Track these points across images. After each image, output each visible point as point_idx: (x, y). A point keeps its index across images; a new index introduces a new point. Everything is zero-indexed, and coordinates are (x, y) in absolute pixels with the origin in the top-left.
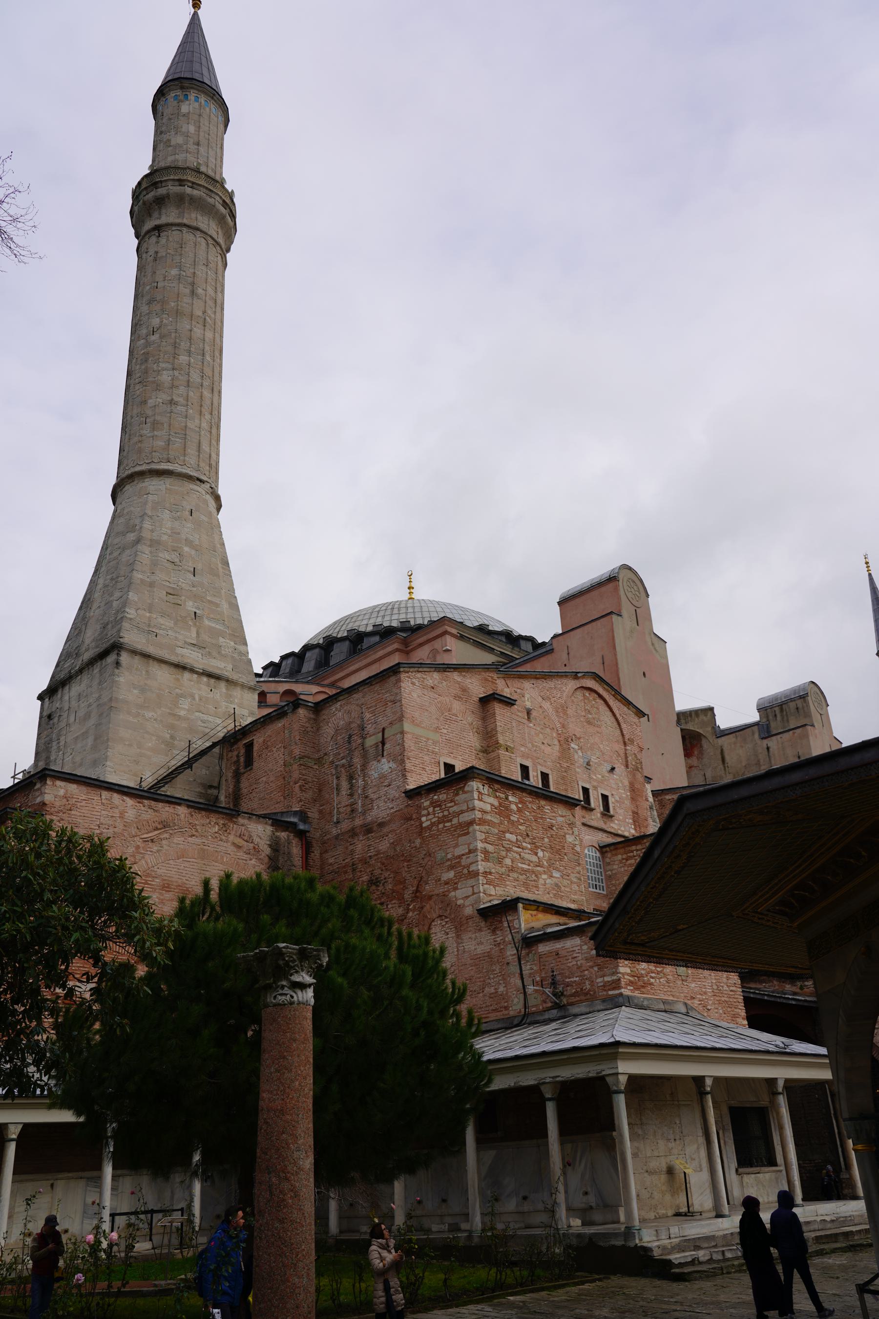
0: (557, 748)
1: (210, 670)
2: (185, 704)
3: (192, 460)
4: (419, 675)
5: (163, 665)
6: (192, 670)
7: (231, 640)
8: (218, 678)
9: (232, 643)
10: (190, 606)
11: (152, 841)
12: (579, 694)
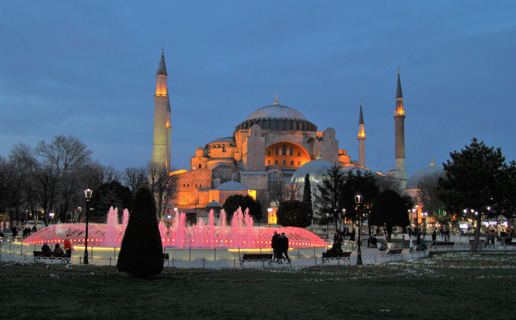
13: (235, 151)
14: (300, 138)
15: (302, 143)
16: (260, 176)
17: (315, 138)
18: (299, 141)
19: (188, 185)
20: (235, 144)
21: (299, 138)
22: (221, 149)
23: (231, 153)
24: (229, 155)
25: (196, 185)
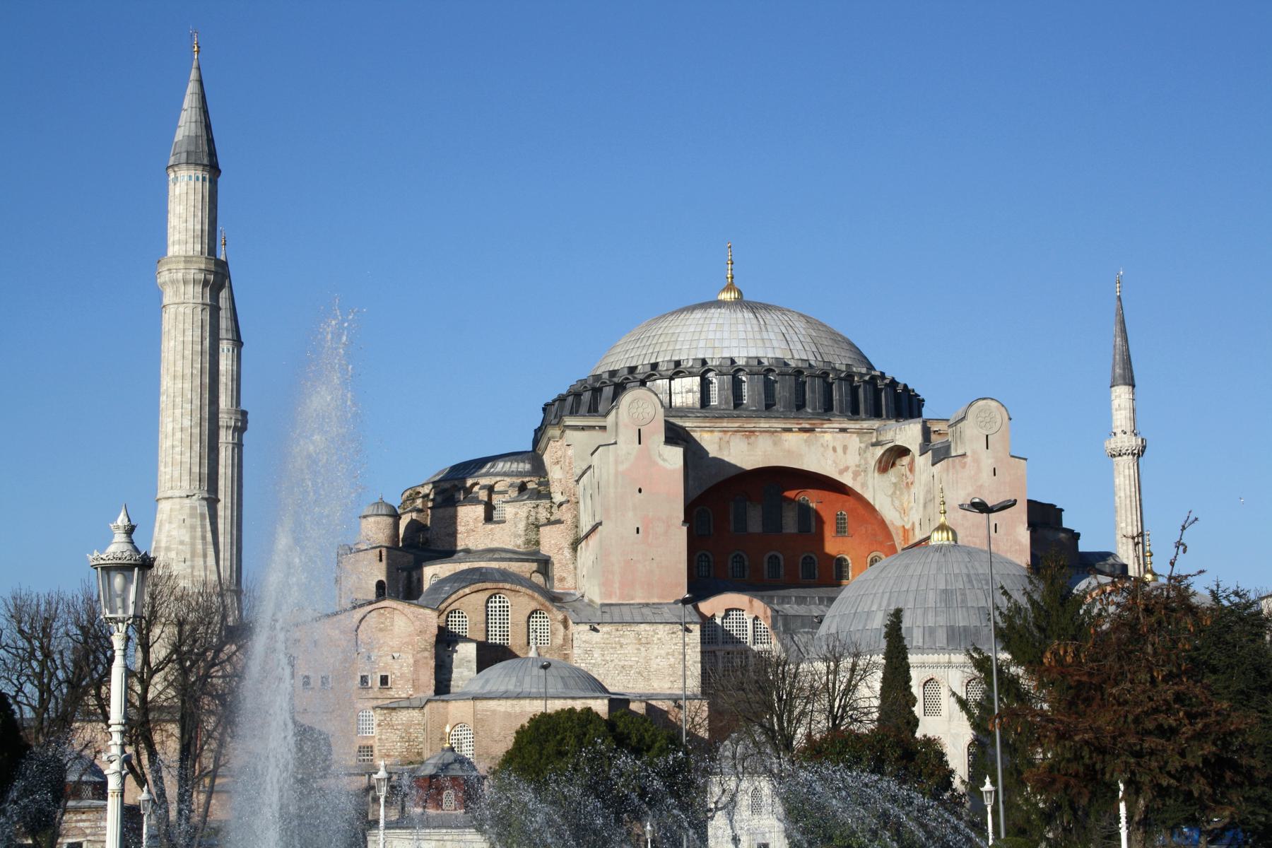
13: (543, 515)
14: (845, 448)
15: (856, 475)
18: (842, 467)
20: (540, 484)
21: (839, 450)
22: (480, 510)
23: (528, 524)
24: (520, 536)
25: (364, 679)
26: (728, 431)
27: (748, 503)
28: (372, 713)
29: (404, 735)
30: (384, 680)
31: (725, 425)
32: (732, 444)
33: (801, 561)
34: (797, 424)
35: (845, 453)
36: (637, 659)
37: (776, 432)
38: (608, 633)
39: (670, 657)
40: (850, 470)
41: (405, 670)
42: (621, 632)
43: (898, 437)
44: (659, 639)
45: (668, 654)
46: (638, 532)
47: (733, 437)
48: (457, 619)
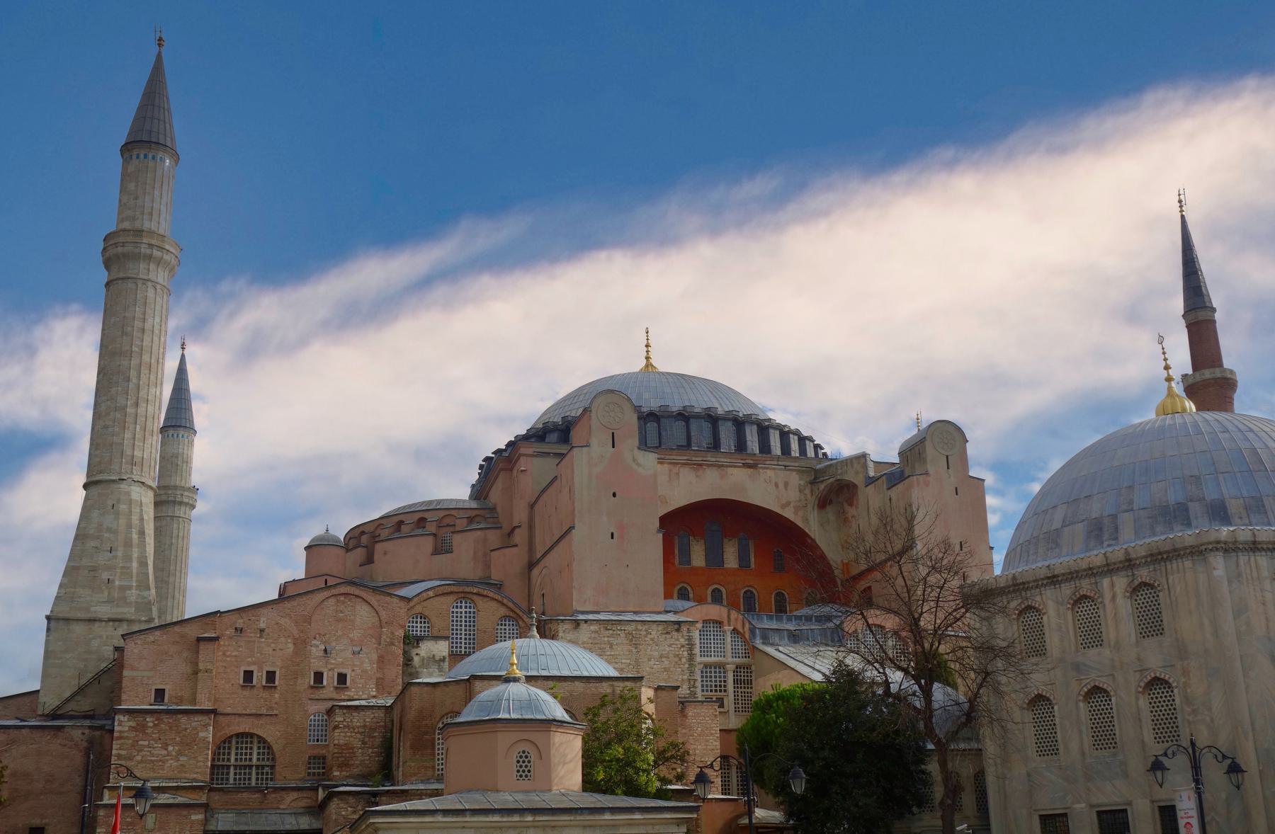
0: (292, 649)
1: (114, 616)
2: (95, 643)
3: (116, 467)
4: (142, 637)
5: (80, 622)
6: (100, 620)
7: (136, 590)
8: (120, 620)
9: (138, 592)
10: (105, 576)
11: (6, 751)
12: (332, 601)
15: (797, 510)
16: (655, 632)
17: (858, 480)
18: (784, 502)
19: (271, 676)
21: (781, 486)
22: (428, 544)
25: (319, 676)
26: (677, 464)
27: (691, 538)
28: (325, 717)
29: (367, 739)
30: (342, 678)
31: (675, 457)
32: (681, 475)
33: (742, 595)
34: (742, 459)
35: (786, 489)
36: (628, 661)
37: (723, 466)
38: (596, 632)
39: (664, 659)
40: (792, 505)
41: (367, 666)
42: (611, 632)
43: (839, 471)
44: (652, 639)
45: (661, 657)
46: (612, 538)
47: (681, 470)
48: (419, 625)
